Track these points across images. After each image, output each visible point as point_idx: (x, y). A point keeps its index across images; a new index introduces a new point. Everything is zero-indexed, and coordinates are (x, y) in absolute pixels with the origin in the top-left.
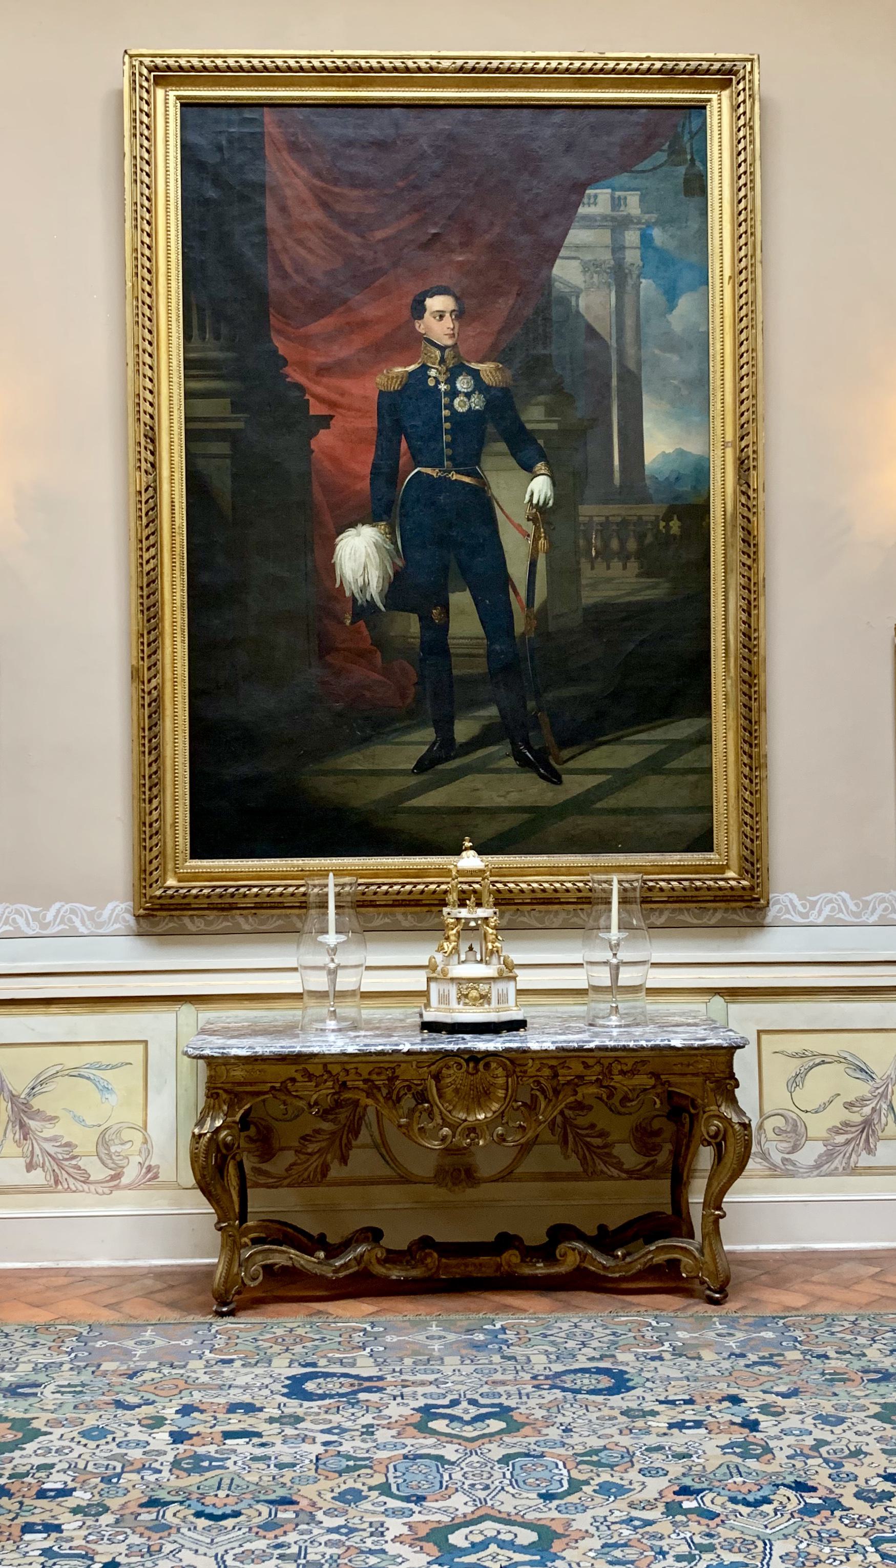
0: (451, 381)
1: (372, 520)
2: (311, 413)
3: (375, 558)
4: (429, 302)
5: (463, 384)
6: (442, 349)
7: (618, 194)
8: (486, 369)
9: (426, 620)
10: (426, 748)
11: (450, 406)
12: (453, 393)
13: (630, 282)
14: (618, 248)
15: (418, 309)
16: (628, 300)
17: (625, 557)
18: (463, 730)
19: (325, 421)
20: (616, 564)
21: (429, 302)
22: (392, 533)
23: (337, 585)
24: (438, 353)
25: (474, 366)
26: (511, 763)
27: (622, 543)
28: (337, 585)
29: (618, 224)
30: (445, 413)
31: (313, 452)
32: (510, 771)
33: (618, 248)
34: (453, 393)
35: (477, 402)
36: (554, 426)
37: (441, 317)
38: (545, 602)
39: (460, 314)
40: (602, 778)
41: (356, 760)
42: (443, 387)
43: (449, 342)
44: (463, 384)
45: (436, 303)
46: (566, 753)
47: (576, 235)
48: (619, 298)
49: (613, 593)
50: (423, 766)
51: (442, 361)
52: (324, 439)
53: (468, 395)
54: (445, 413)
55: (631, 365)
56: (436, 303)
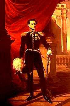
0: (34, 35)
1: (20, 57)
2: (11, 40)
3: (20, 64)
4: (30, 22)
5: (36, 35)
6: (33, 30)
7: (62, 5)
8: (41, 33)
9: (29, 75)
10: (29, 96)
11: (34, 39)
12: (35, 36)
13: (65, 18)
14: (62, 13)
15: (29, 23)
16: (64, 22)
17: (64, 65)
18: (35, 93)
19: (13, 41)
20: (63, 65)
21: (30, 22)
22: (23, 59)
23: (13, 68)
24: (32, 30)
25: (39, 32)
26: (43, 99)
27: (64, 62)
28: (13, 68)
29: (63, 10)
30: (33, 40)
31: (11, 46)
32: (43, 101)
33: (62, 13)
34: (35, 36)
35: (39, 38)
36: (52, 42)
37: (33, 24)
38: (50, 73)
39: (36, 24)
40: (60, 103)
41: (16, 99)
42: (33, 36)
43: (34, 28)
44: (36, 35)
45: (32, 22)
46: (53, 97)
47: (56, 11)
48: (63, 22)
49: (62, 70)
50: (28, 99)
51: (33, 31)
52: (13, 44)
53: (37, 37)
54: (33, 40)
55: (65, 33)
56: (32, 22)
